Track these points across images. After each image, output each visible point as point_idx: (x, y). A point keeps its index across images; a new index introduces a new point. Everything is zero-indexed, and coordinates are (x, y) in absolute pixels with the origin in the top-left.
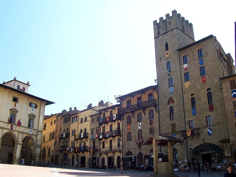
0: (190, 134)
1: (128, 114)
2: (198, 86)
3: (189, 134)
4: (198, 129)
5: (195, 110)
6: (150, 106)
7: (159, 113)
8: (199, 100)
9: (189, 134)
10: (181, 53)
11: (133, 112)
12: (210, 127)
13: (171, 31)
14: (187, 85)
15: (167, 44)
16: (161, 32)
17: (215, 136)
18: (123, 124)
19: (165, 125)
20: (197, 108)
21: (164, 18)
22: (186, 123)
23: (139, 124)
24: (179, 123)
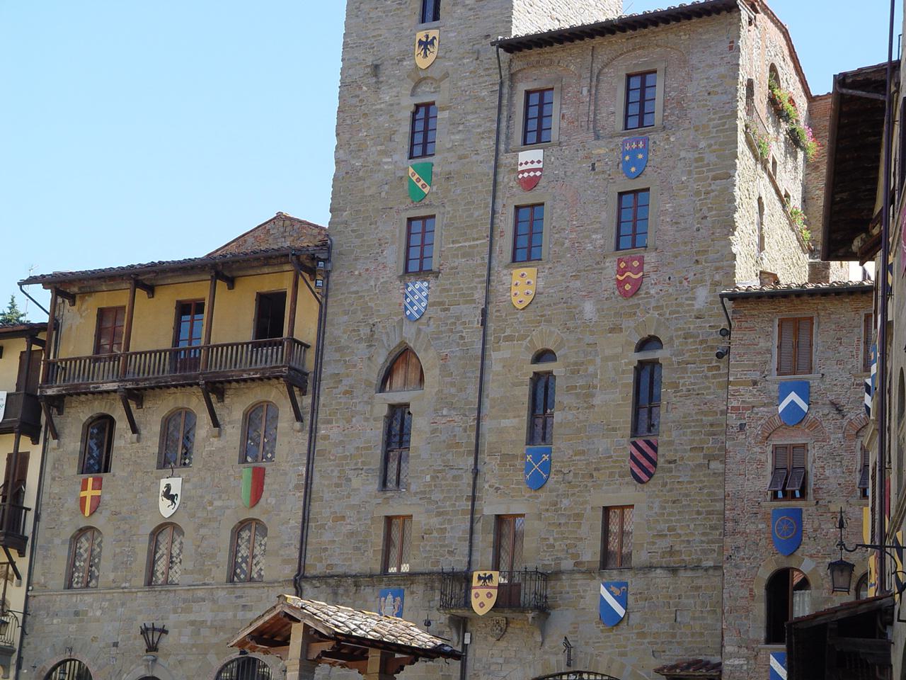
0: (490, 603)
1: (99, 407)
2: (589, 308)
3: (482, 600)
4: (546, 577)
5: (546, 457)
6: (260, 379)
7: (313, 432)
8: (578, 395)
9: (482, 600)
10: (517, 65)
11: (135, 396)
12: (615, 575)
17: (642, 635)
18: (48, 469)
19: (343, 518)
20: (561, 445)
22: (478, 527)
23: (164, 482)
24: (435, 521)
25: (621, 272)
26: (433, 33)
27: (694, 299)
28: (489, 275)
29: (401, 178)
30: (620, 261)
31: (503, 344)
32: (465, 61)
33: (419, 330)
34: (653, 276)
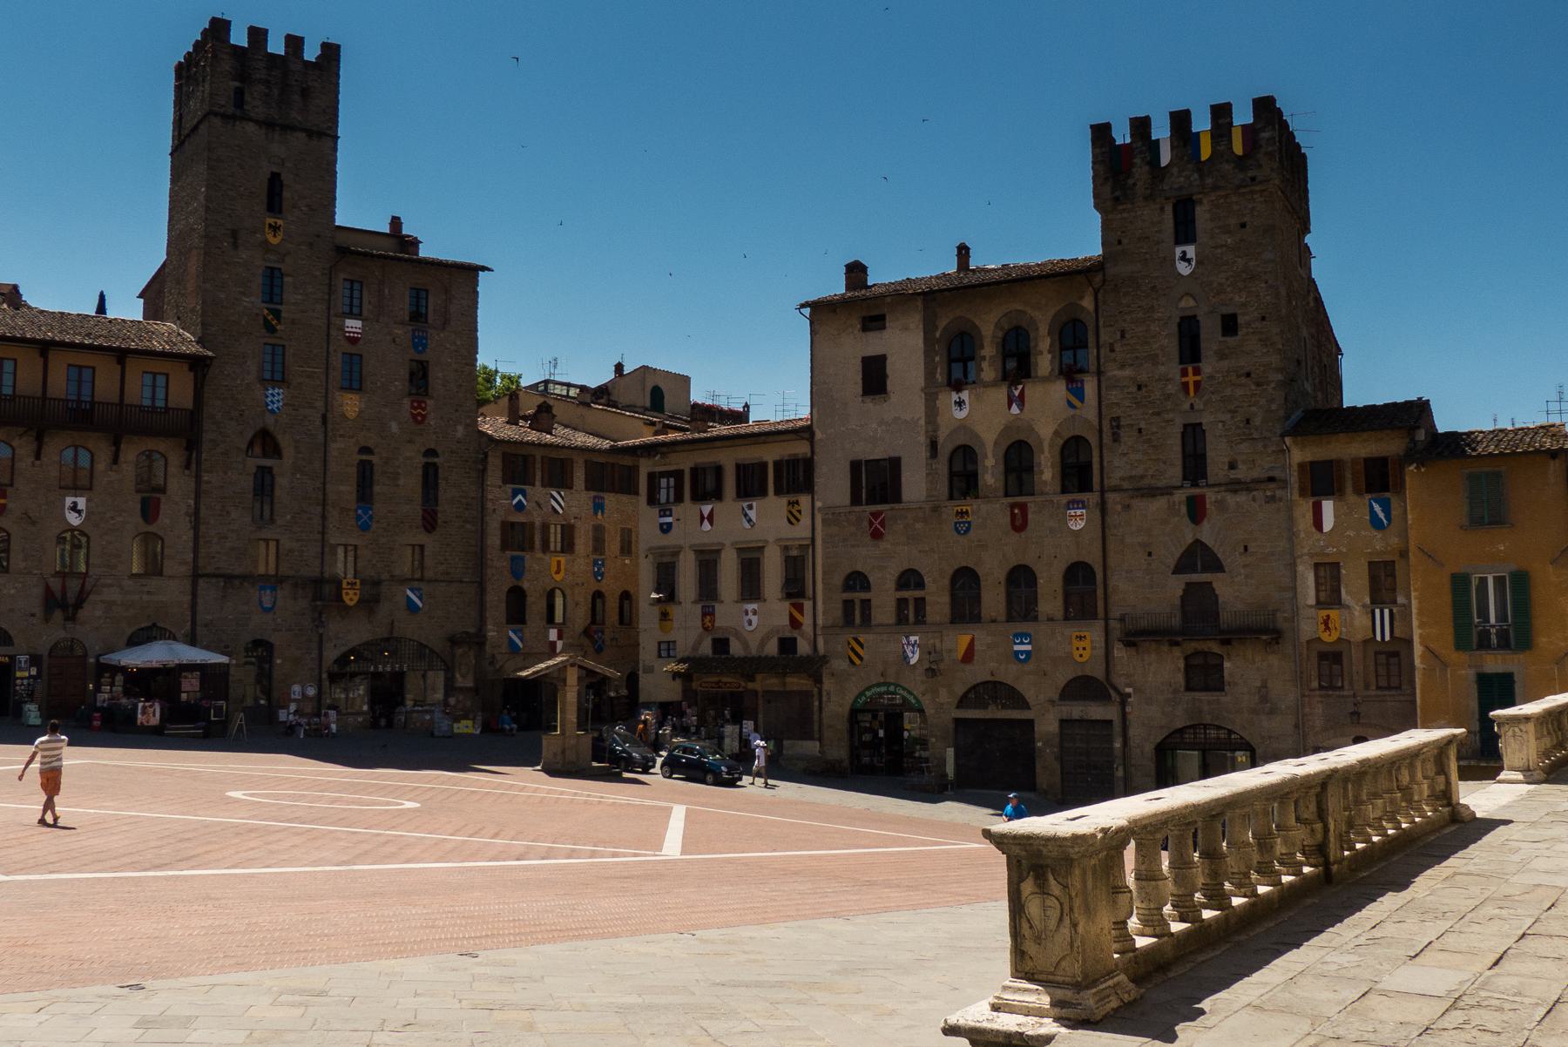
0: (356, 599)
2: (394, 427)
4: (377, 583)
5: (371, 512)
13: (310, 133)
14: (351, 405)
15: (275, 182)
16: (256, 104)
21: (276, 46)
22: (327, 550)
25: (415, 408)
26: (280, 222)
27: (457, 431)
28: (327, 393)
29: (257, 314)
30: (413, 402)
31: (338, 439)
32: (303, 247)
33: (276, 421)
34: (432, 414)
